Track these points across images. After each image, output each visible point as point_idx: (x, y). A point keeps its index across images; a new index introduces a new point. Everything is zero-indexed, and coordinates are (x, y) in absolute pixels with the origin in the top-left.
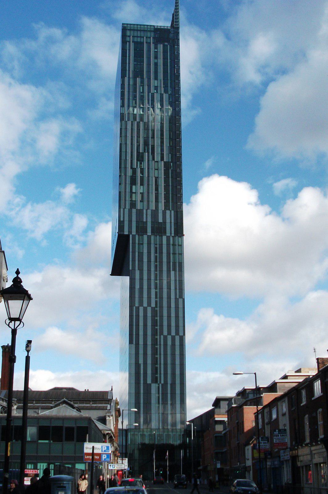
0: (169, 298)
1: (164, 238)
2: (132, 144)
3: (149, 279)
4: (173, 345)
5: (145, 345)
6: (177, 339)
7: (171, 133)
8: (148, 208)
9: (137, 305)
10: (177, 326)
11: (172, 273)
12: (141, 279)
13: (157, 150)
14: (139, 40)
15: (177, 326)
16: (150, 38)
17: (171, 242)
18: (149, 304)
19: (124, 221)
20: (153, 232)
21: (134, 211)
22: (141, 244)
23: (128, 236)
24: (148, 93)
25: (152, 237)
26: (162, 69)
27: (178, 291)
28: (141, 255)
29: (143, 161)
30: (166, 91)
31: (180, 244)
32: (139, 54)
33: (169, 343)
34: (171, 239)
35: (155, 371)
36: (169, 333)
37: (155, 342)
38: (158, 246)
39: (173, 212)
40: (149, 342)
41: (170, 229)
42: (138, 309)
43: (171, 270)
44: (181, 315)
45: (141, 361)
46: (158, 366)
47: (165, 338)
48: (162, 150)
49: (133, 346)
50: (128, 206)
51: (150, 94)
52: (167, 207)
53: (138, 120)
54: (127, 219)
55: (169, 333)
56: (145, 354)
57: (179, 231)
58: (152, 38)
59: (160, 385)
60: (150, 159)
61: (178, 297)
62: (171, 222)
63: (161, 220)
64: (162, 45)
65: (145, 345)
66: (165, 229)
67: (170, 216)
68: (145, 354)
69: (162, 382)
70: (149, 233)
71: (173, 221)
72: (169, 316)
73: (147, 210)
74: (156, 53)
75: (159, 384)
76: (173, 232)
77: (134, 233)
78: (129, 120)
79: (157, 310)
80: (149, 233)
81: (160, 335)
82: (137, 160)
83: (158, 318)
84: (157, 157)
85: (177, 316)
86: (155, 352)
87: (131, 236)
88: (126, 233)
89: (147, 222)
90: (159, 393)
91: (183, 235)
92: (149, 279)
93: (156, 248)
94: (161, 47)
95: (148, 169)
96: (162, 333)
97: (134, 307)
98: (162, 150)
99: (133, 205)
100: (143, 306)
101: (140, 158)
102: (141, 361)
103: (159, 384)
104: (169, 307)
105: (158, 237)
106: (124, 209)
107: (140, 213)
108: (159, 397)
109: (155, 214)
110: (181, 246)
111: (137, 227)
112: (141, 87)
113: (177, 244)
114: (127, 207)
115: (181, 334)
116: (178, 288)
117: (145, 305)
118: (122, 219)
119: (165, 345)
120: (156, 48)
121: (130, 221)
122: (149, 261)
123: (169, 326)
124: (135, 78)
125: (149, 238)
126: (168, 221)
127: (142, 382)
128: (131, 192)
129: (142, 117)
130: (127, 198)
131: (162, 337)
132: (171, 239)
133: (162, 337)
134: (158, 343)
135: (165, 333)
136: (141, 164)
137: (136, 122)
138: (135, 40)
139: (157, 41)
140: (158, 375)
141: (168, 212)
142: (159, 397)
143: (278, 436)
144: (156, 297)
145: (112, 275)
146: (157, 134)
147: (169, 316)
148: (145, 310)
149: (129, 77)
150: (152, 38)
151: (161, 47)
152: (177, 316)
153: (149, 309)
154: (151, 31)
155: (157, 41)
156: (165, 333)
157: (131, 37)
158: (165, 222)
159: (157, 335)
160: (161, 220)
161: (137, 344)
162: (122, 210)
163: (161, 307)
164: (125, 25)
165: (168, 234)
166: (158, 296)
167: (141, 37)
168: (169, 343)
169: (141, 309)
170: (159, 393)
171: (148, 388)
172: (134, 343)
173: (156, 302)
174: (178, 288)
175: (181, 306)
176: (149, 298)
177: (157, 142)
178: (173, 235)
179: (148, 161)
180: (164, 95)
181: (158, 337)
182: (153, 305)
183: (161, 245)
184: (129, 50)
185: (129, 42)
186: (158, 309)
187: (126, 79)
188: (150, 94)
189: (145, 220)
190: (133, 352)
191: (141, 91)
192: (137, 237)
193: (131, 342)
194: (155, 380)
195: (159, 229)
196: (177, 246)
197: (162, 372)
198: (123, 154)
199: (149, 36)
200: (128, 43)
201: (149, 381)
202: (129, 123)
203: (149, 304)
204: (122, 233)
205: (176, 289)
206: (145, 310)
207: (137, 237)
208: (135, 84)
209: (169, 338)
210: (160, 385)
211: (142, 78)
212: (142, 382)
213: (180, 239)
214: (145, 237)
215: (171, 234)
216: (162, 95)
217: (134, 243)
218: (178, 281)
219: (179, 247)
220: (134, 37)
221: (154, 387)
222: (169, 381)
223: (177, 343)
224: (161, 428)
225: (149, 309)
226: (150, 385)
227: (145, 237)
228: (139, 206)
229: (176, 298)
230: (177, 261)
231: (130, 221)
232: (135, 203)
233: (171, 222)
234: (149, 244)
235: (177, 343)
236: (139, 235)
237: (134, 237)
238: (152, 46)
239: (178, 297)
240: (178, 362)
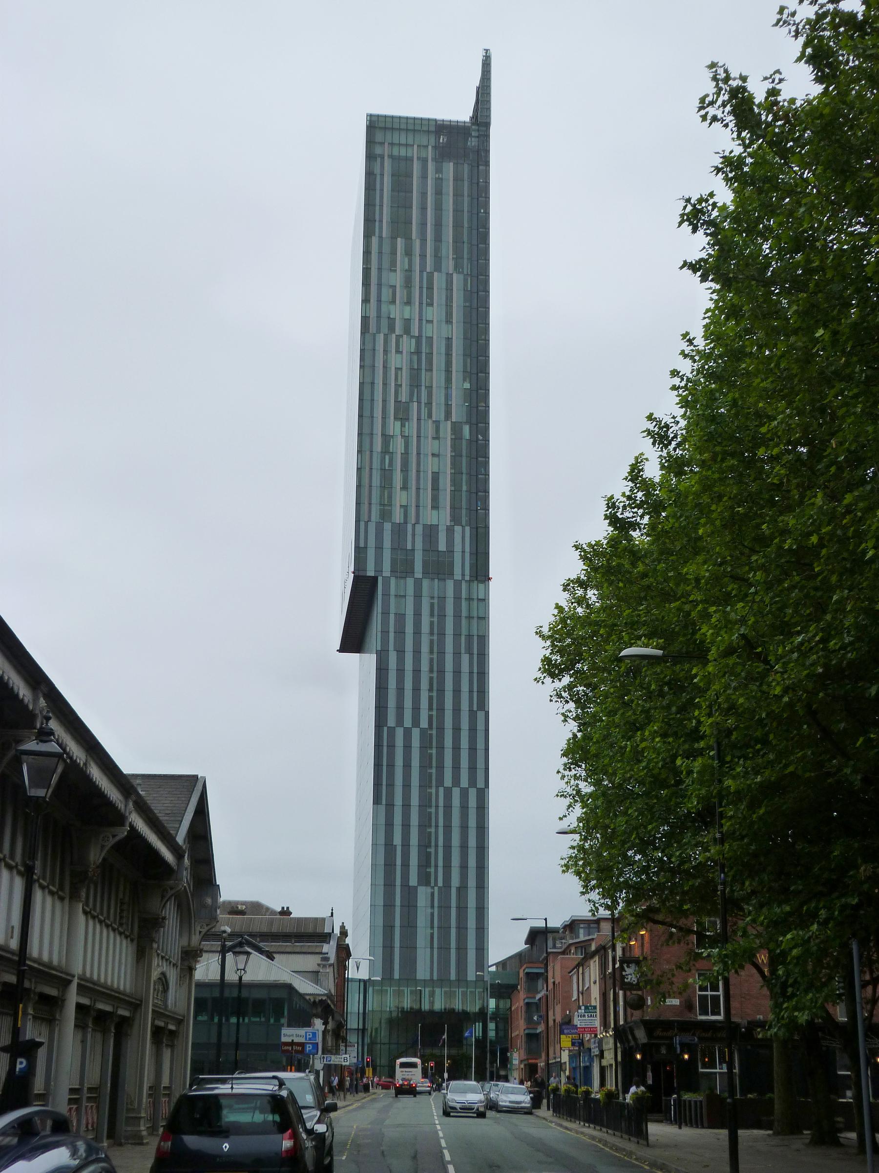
0: (457, 710)
1: (450, 584)
2: (385, 384)
3: (417, 672)
4: (464, 808)
5: (406, 806)
6: (472, 793)
7: (469, 360)
8: (417, 522)
9: (391, 721)
10: (473, 768)
11: (465, 658)
12: (401, 671)
13: (438, 397)
14: (403, 152)
15: (473, 768)
16: (427, 146)
17: (464, 595)
18: (416, 722)
19: (366, 548)
20: (425, 573)
21: (387, 526)
22: (401, 597)
23: (375, 579)
24: (421, 272)
25: (426, 583)
26: (451, 219)
27: (475, 694)
28: (401, 618)
29: (407, 419)
30: (458, 267)
31: (481, 596)
32: (401, 185)
33: (456, 802)
34: (464, 586)
35: (425, 861)
36: (456, 781)
37: (426, 803)
38: (436, 601)
39: (467, 529)
40: (415, 801)
41: (461, 566)
42: (392, 731)
43: (463, 651)
44: (480, 745)
45: (397, 840)
46: (432, 850)
47: (448, 793)
48: (448, 397)
49: (382, 808)
50: (375, 517)
51: (425, 273)
53: (398, 331)
54: (372, 543)
55: (456, 781)
56: (406, 826)
57: (480, 571)
58: (430, 148)
59: (436, 888)
60: (423, 417)
61: (475, 708)
62: (463, 552)
63: (442, 547)
64: (451, 164)
65: (406, 806)
66: (451, 564)
67: (462, 538)
68: (406, 826)
69: (440, 884)
70: (418, 574)
71: (467, 549)
72: (456, 748)
73: (414, 525)
74: (439, 182)
75: (433, 888)
76: (467, 572)
77: (387, 572)
78: (379, 331)
79: (431, 735)
80: (418, 574)
81: (437, 787)
82: (396, 418)
83: (434, 751)
84: (438, 413)
85: (473, 749)
86: (425, 823)
87: (380, 579)
88: (371, 573)
89: (413, 550)
90: (432, 907)
91: (489, 579)
92: (417, 672)
93: (432, 605)
94: (449, 168)
95: (419, 437)
96: (440, 782)
97: (385, 729)
98: (448, 397)
100: (403, 726)
101: (402, 415)
102: (397, 840)
103: (433, 888)
104: (457, 729)
105: (436, 580)
106: (366, 523)
107: (399, 531)
108: (432, 915)
109: (431, 532)
110: (484, 601)
111: (394, 562)
112: (406, 260)
113: (475, 597)
114: (373, 518)
115: (480, 784)
116: (475, 689)
117: (408, 723)
118: (362, 545)
119: (448, 807)
120: (439, 170)
121: (379, 548)
122: (417, 632)
123: (456, 767)
124: (393, 238)
125: (418, 584)
126: (458, 548)
127: (398, 882)
129: (407, 323)
130: (374, 501)
131: (441, 790)
132: (464, 586)
133: (441, 790)
134: (434, 804)
135: (448, 782)
136: (403, 426)
137: (394, 336)
138: (395, 152)
139: (443, 154)
140: (432, 870)
141: (458, 529)
142: (432, 915)
143: (584, 1016)
144: (430, 709)
145: (341, 651)
146: (438, 361)
147: (456, 748)
148: (408, 733)
149: (381, 237)
150: (430, 148)
151: (449, 168)
152: (473, 749)
153: (416, 733)
154: (428, 132)
155: (443, 154)
156: (448, 782)
157: (386, 144)
158: (450, 551)
159: (431, 787)
160: (442, 547)
161: (390, 806)
162: (362, 524)
163: (441, 729)
164: (373, 119)
165: (458, 576)
166: (435, 706)
167: (407, 145)
168: (456, 802)
169: (400, 732)
170: (432, 907)
171: (410, 894)
172: (384, 802)
173: (430, 718)
174: (475, 689)
175: (480, 726)
176: (416, 709)
177: (437, 377)
178: (467, 578)
179: (419, 420)
180: (455, 276)
181: (433, 791)
182: (424, 724)
183: (442, 599)
184: (382, 175)
185: (382, 157)
186: (434, 732)
187: (375, 240)
188: (425, 274)
189: (409, 547)
190: (382, 820)
191: (407, 267)
192: (393, 581)
193: (377, 801)
194: (425, 879)
195: (439, 567)
196: (475, 602)
197: (441, 863)
198: (367, 405)
199: (425, 143)
200: (379, 160)
201: (413, 881)
202: (380, 338)
203: (416, 722)
204: (361, 573)
205: (471, 691)
206: (408, 733)
207: (393, 581)
208: (394, 252)
209: (456, 792)
210: (436, 888)
211: (408, 238)
212: (398, 882)
213: (481, 586)
214: (410, 582)
215: (463, 575)
216: (449, 277)
217: (386, 595)
218: (475, 675)
219: (481, 604)
220: (392, 144)
221: (423, 894)
222: (455, 882)
223: (472, 802)
224: (435, 978)
225: (416, 733)
226: (416, 888)
227: (410, 582)
228: (398, 516)
229: (471, 710)
230: (475, 633)
231: (379, 548)
232: (390, 512)
233: (463, 552)
234: (418, 596)
235: (472, 802)
236: (397, 577)
237: (387, 581)
238: (431, 166)
239: (475, 708)
240: (472, 842)
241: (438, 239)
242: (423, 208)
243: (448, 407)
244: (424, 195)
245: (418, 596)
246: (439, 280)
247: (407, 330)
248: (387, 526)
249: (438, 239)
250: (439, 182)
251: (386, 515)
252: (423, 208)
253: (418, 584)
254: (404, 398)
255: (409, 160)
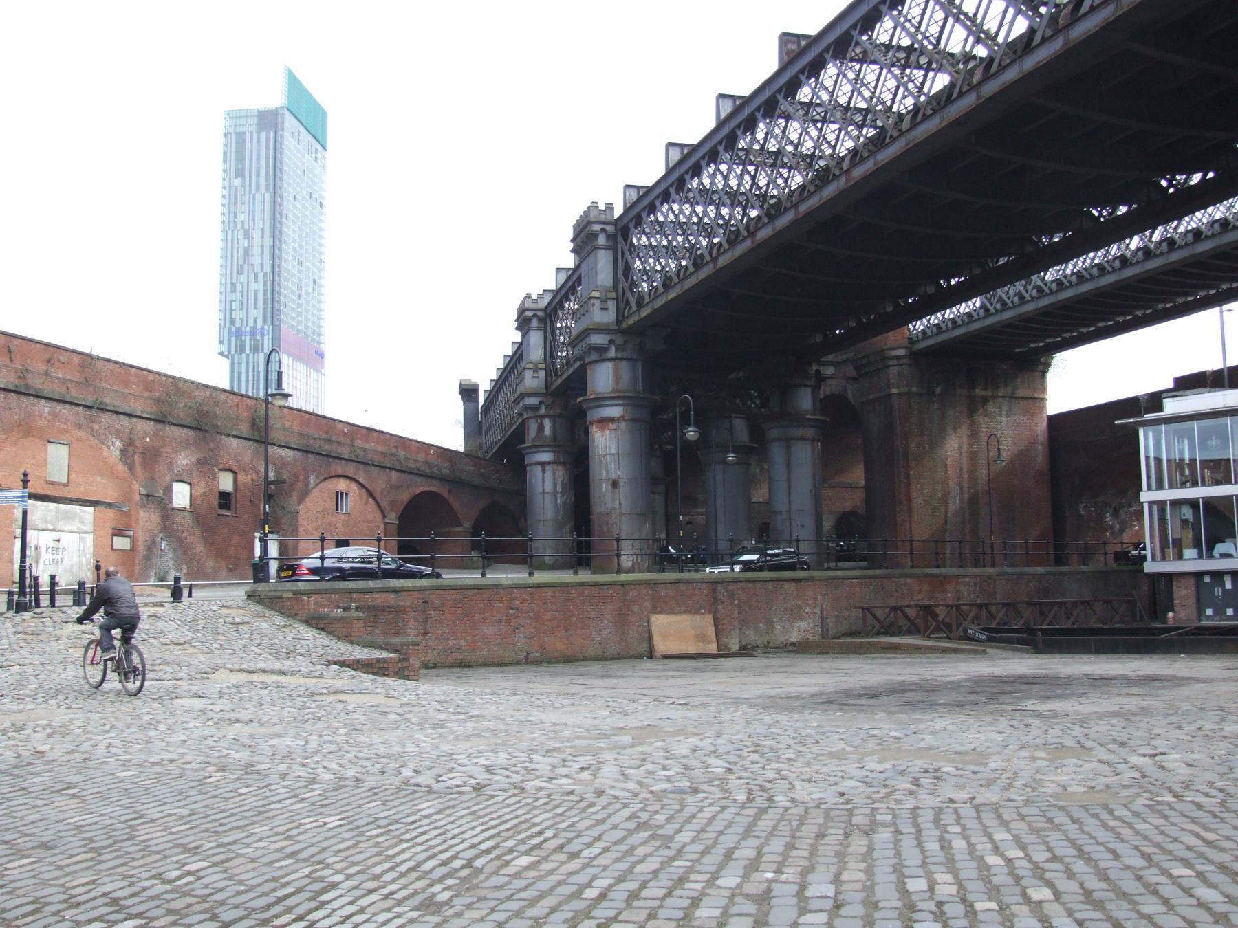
28: (240, 374)
52: (264, 321)
70: (247, 351)
74: (259, 141)
80: (247, 351)
84: (258, 269)
94: (263, 135)
99: (232, 322)
122: (247, 381)
125: (247, 356)
128: (231, 310)
151: (263, 135)
211: (243, 176)
234: (247, 363)
238: (255, 135)
241: (258, 175)
242: (251, 159)
243: (262, 265)
244: (251, 152)
245: (247, 363)
246: (259, 197)
247: (243, 227)
248: (233, 329)
249: (258, 175)
250: (259, 141)
251: (232, 322)
252: (251, 159)
253: (247, 356)
254: (241, 262)
255: (244, 133)
